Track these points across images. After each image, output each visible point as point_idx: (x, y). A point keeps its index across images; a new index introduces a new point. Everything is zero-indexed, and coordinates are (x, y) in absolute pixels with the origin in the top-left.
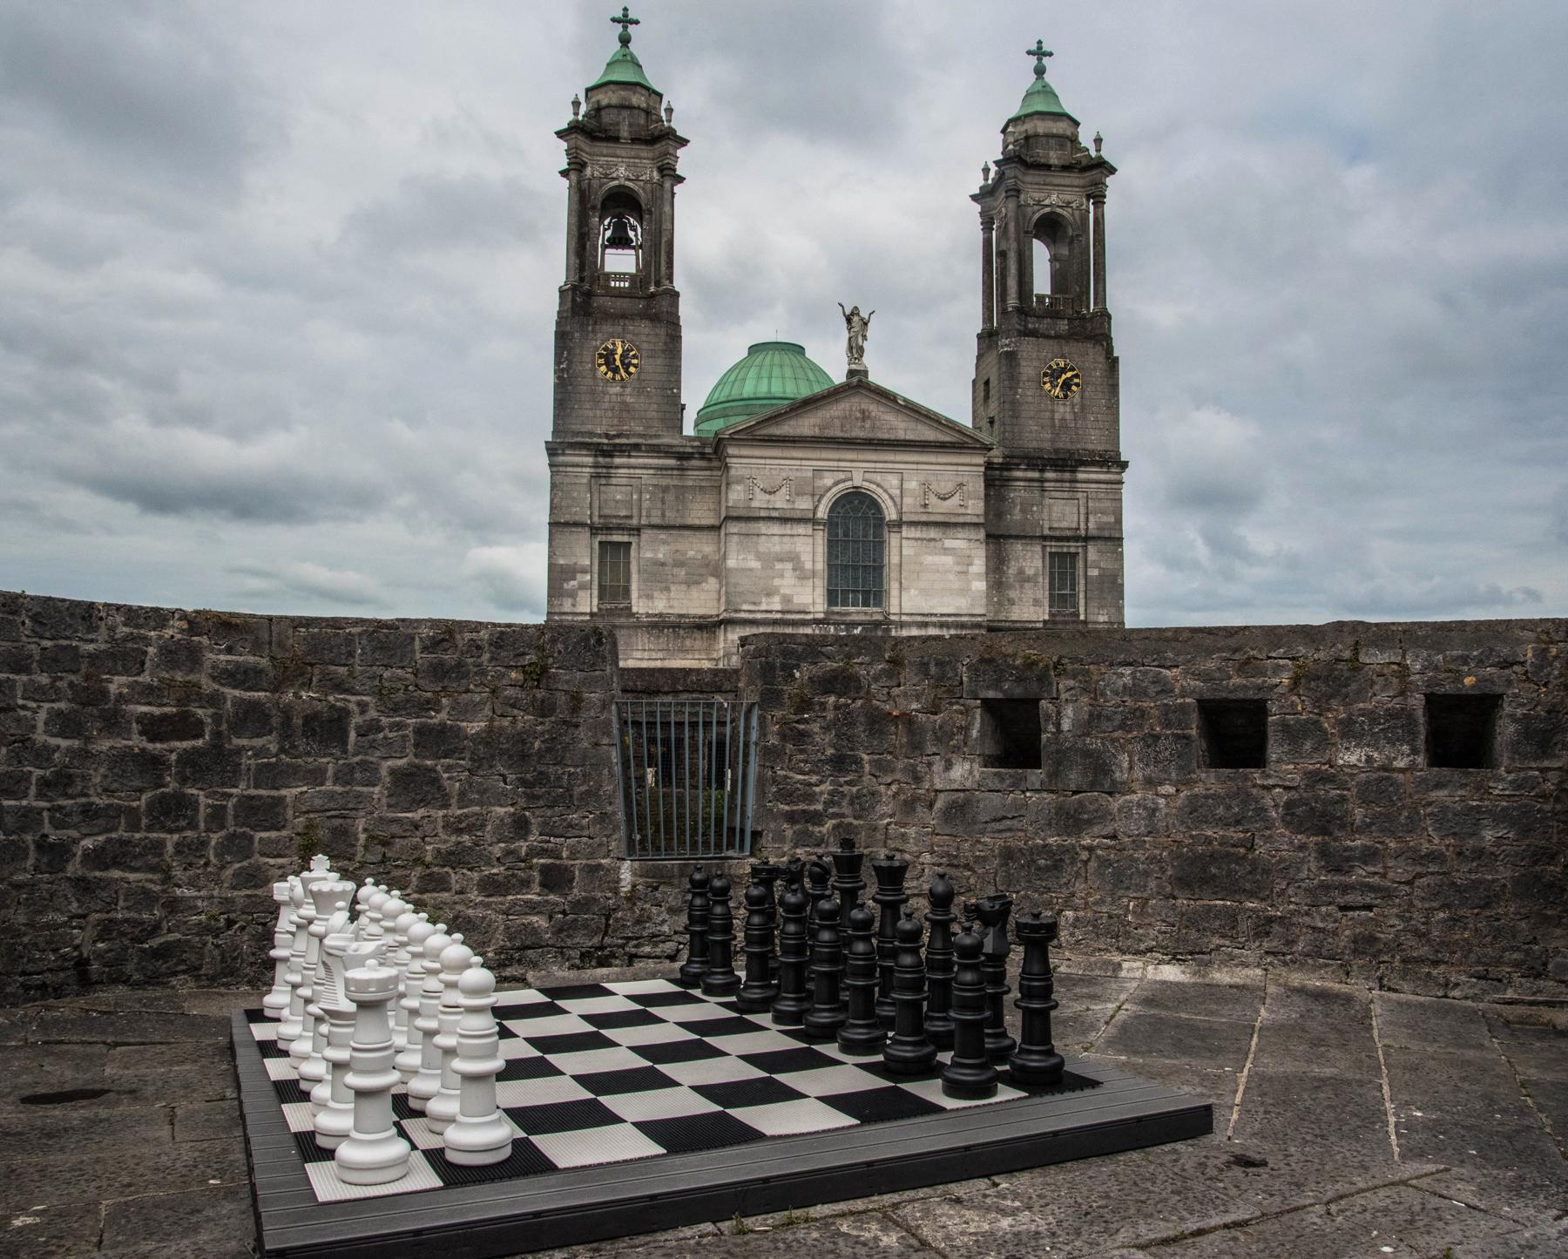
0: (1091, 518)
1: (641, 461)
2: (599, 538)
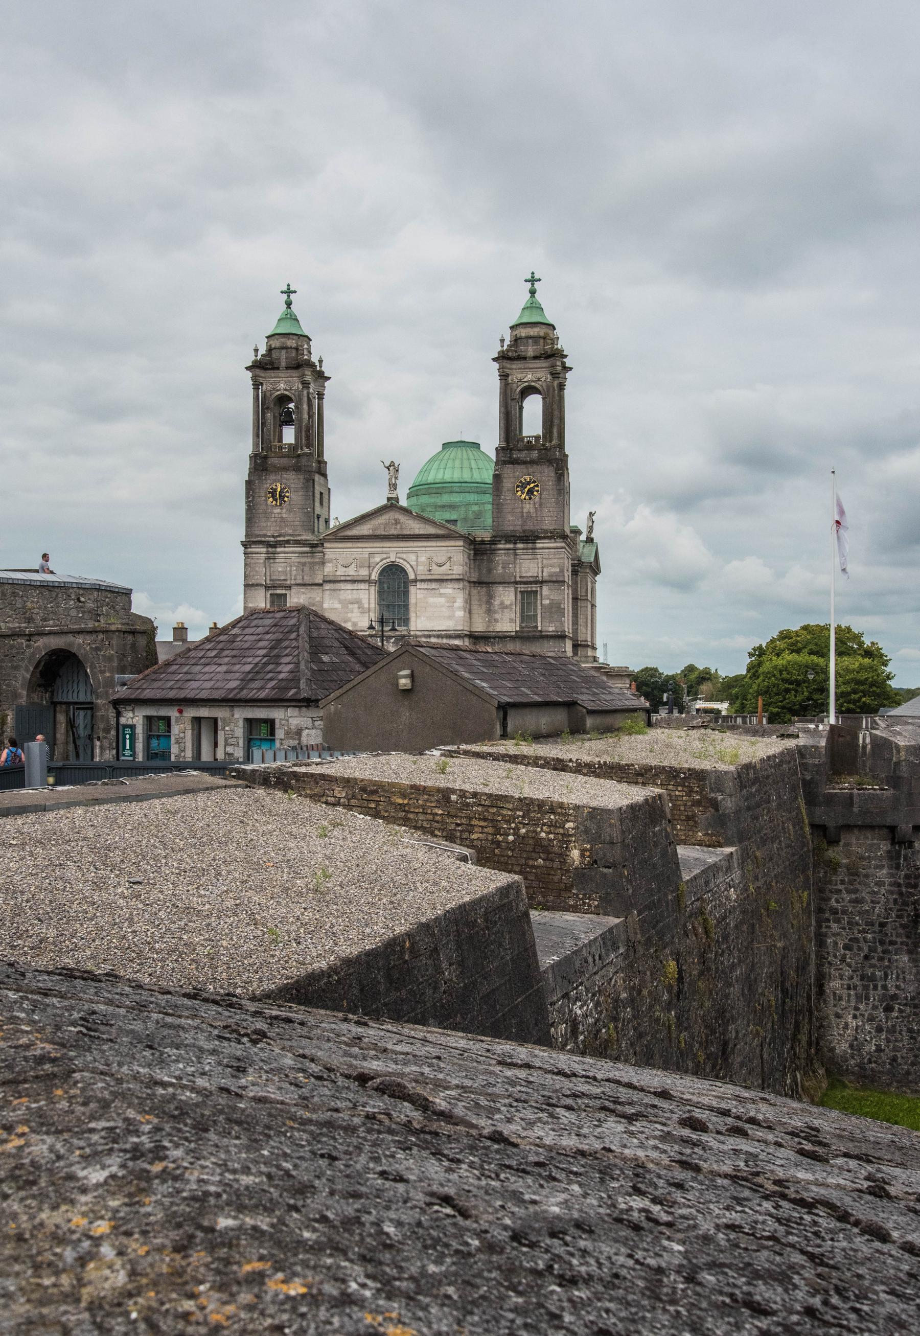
0: (545, 570)
1: (291, 549)
2: (270, 592)
